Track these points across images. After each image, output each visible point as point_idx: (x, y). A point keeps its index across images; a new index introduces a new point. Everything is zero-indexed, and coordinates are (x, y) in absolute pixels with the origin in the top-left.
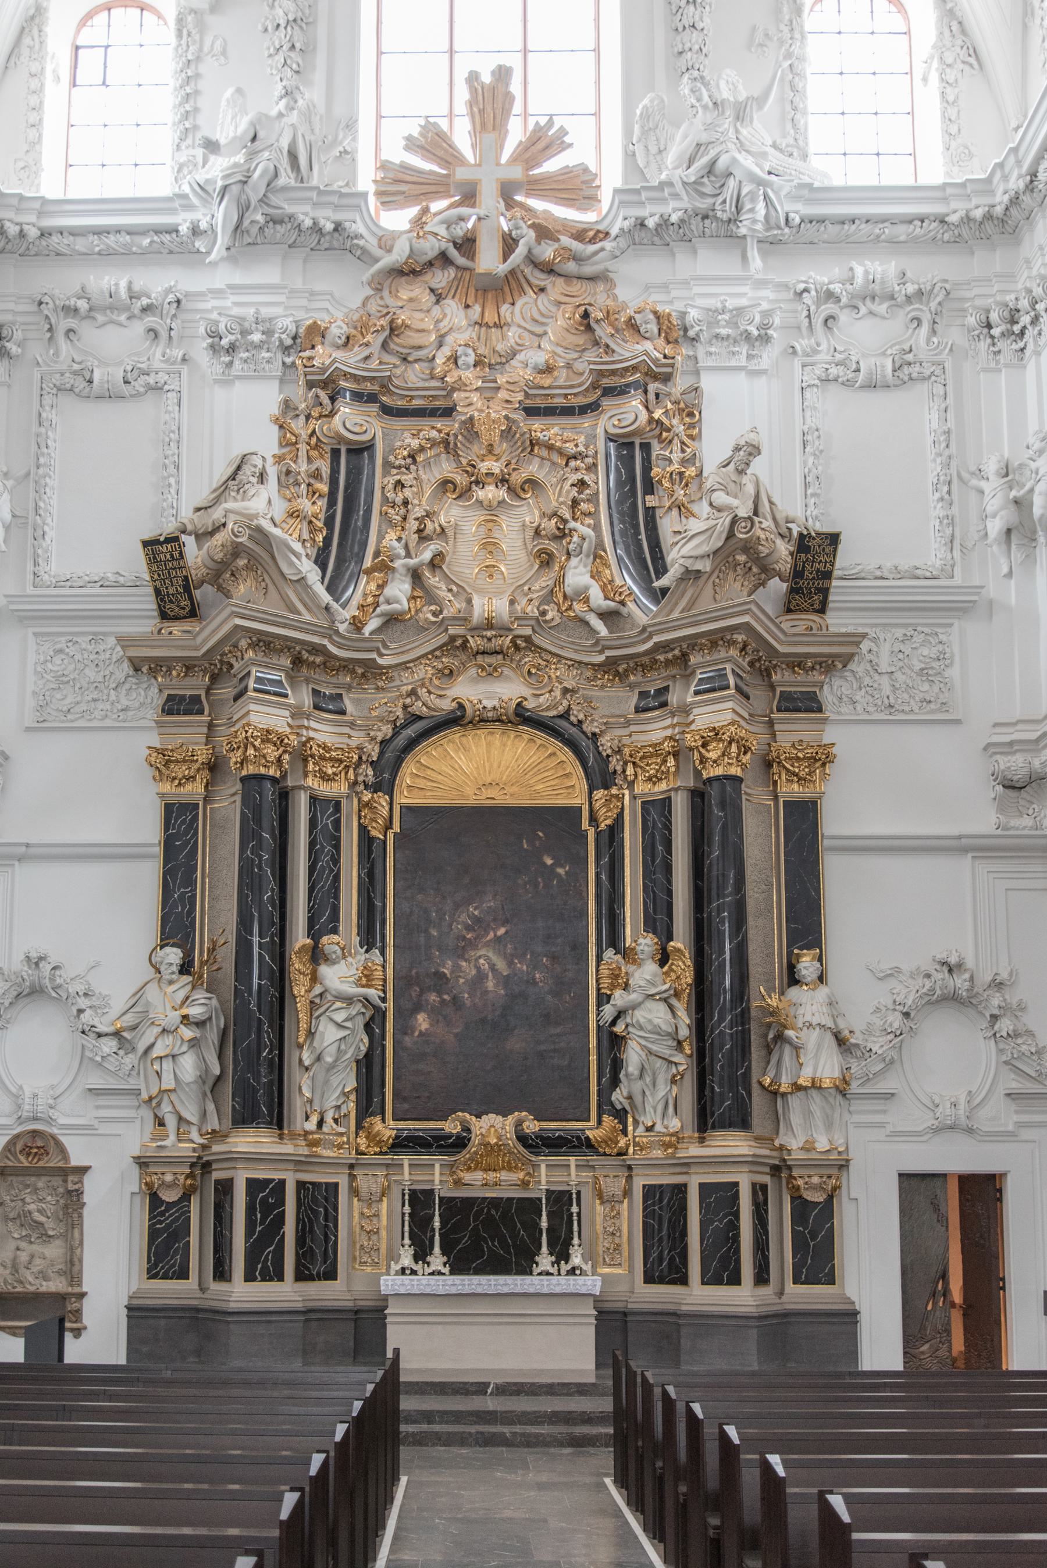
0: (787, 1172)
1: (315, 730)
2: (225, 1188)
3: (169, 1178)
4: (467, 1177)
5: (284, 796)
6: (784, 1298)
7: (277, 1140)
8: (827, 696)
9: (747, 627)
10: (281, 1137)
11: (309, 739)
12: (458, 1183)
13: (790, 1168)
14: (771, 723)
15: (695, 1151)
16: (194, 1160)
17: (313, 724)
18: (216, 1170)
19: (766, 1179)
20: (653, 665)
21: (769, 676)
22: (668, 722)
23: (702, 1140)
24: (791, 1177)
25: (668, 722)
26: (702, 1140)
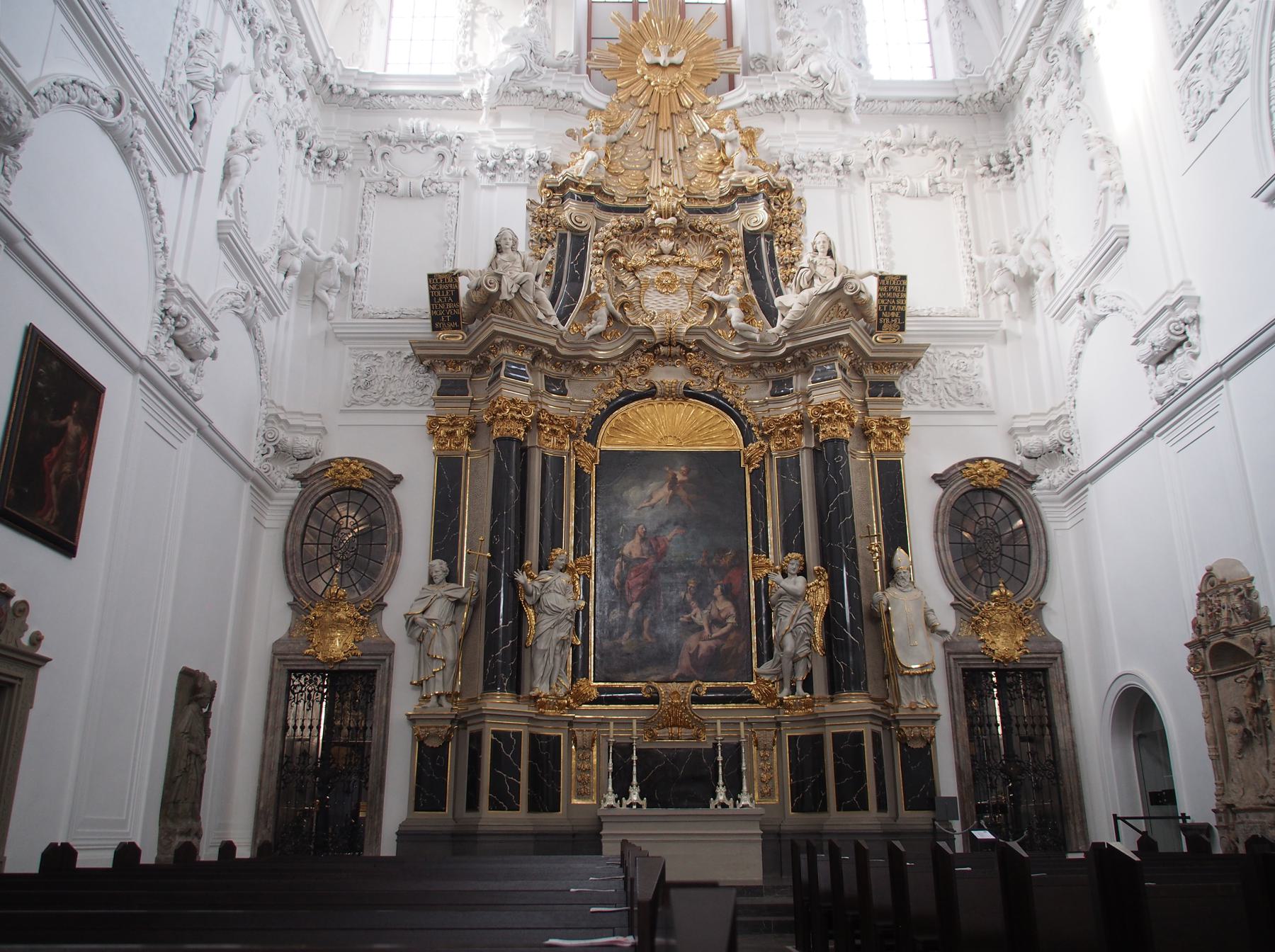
0: (896, 726)
1: (547, 404)
2: (476, 738)
3: (433, 730)
4: (660, 733)
5: (524, 452)
6: (898, 822)
7: (516, 701)
8: (903, 385)
9: (848, 337)
10: (518, 699)
11: (542, 410)
12: (654, 737)
13: (897, 722)
14: (865, 404)
15: (829, 708)
16: (453, 717)
17: (544, 400)
18: (469, 725)
19: (879, 729)
20: (784, 364)
21: (861, 372)
22: (795, 401)
23: (832, 700)
24: (900, 730)
25: (795, 401)
26: (832, 700)
